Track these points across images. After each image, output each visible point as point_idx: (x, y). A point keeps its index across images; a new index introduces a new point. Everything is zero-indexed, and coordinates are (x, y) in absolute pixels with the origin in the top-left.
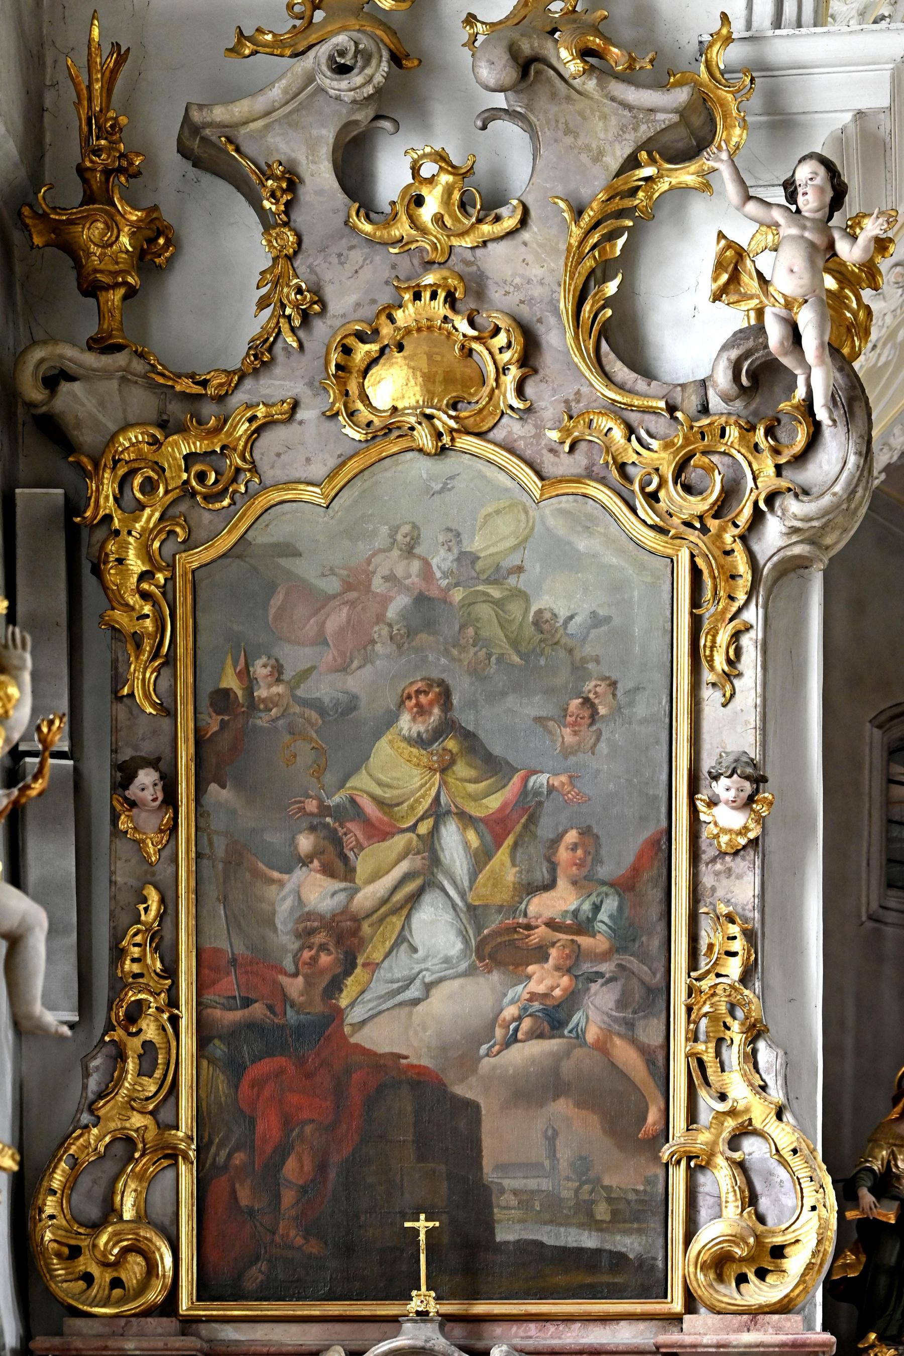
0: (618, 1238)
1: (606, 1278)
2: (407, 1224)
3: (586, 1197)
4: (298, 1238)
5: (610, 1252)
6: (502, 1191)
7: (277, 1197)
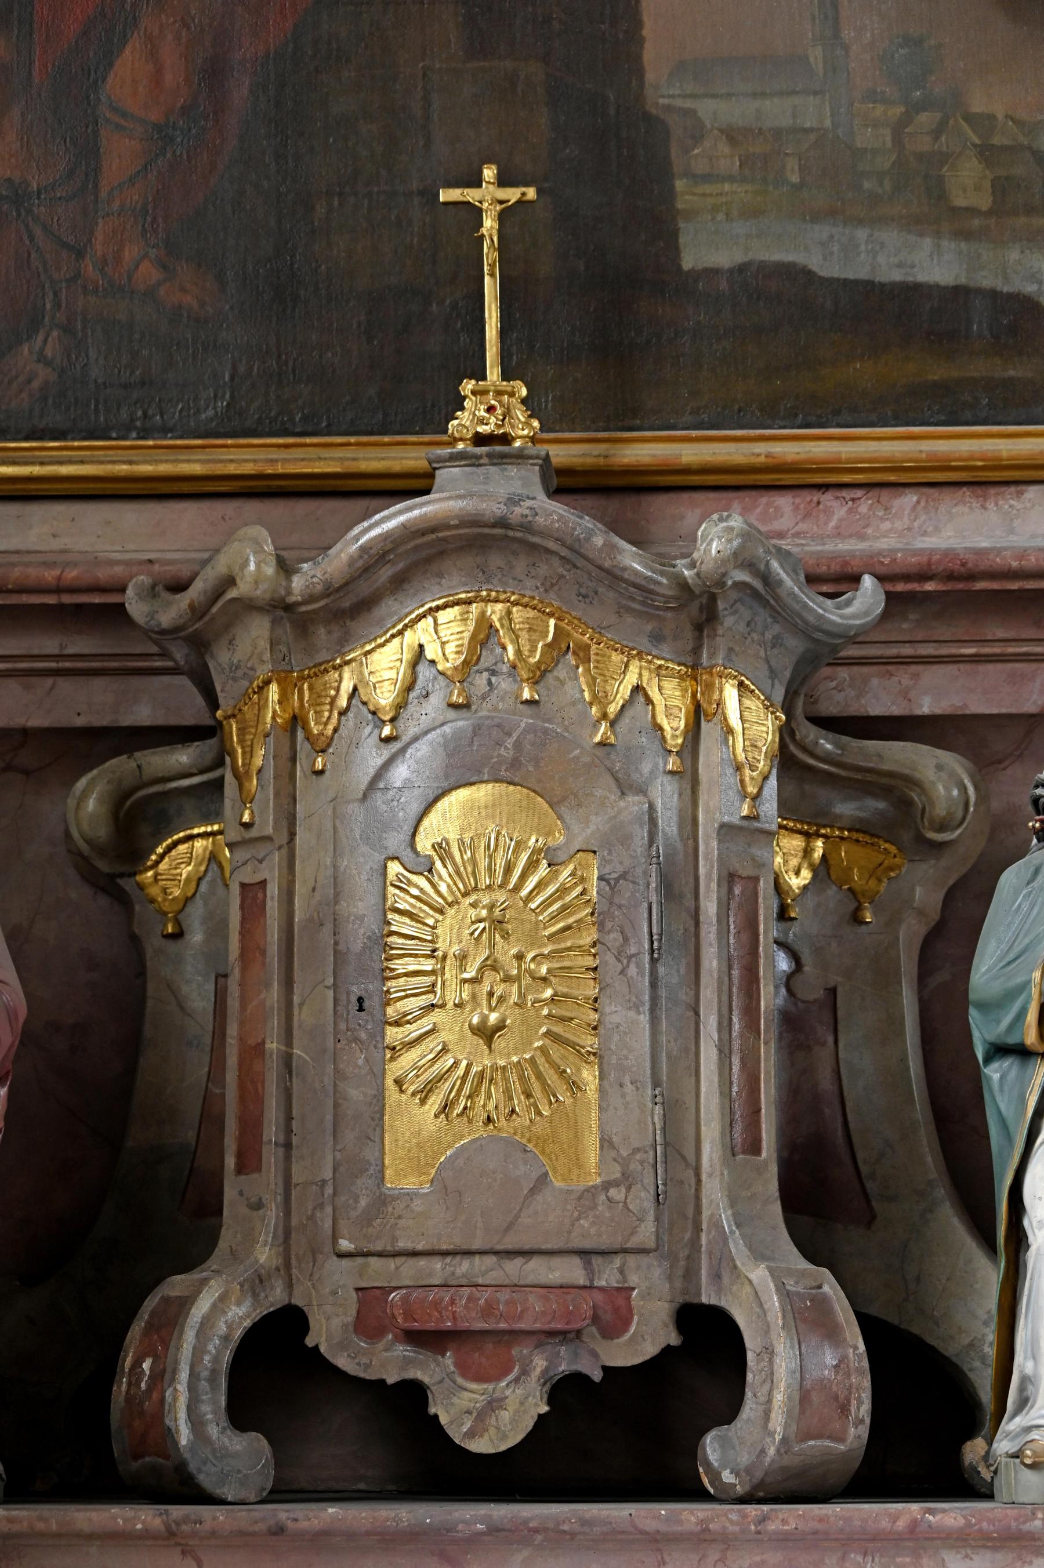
0: (1013, 255)
1: (980, 368)
2: (446, 195)
3: (924, 144)
4: (145, 267)
5: (994, 294)
6: (698, 134)
7: (88, 155)
